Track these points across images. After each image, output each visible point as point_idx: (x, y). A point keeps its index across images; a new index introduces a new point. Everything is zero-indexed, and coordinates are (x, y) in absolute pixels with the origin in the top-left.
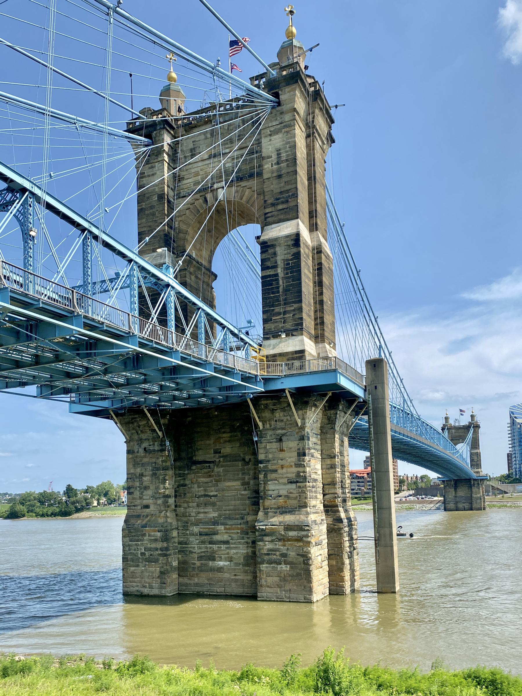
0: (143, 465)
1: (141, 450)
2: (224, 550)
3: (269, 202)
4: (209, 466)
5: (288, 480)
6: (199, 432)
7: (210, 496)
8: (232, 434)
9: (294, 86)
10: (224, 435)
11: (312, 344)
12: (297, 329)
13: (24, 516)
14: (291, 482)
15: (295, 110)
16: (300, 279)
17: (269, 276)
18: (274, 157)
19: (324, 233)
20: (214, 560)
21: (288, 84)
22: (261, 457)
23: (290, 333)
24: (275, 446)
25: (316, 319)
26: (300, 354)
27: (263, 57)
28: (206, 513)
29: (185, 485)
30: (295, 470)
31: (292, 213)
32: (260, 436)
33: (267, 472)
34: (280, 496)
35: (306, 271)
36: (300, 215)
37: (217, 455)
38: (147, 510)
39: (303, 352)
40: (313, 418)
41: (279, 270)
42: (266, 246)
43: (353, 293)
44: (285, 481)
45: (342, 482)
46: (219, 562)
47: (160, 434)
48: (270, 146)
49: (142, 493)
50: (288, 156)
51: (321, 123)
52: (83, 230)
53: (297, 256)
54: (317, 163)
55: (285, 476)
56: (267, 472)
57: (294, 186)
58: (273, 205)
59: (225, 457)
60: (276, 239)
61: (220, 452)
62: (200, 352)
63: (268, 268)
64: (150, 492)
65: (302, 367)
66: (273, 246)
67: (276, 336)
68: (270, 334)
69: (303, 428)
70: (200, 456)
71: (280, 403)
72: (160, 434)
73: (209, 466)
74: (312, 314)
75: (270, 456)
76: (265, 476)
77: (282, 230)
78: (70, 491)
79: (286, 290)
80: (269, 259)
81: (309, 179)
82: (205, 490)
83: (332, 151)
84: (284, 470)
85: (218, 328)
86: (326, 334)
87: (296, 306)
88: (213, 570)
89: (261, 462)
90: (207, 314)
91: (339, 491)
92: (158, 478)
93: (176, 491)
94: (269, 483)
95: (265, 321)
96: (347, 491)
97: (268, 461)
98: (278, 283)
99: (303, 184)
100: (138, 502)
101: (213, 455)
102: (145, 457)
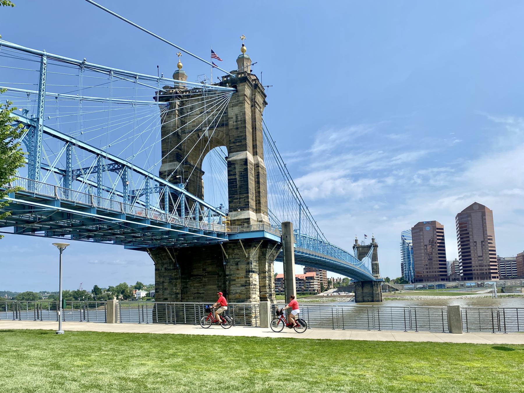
0: (164, 277)
1: (163, 269)
3: (232, 141)
7: (200, 293)
9: (244, 83)
10: (208, 261)
11: (254, 214)
12: (246, 207)
14: (243, 286)
15: (245, 95)
16: (248, 182)
17: (232, 179)
18: (234, 118)
19: (262, 156)
21: (241, 82)
22: (227, 273)
23: (242, 209)
24: (235, 267)
25: (256, 201)
26: (248, 220)
27: (229, 66)
29: (187, 288)
30: (244, 279)
31: (244, 148)
32: (227, 262)
33: (230, 280)
35: (251, 177)
36: (248, 148)
39: (249, 219)
40: (254, 253)
41: (237, 177)
42: (230, 165)
43: (282, 176)
45: (269, 285)
47: (174, 260)
48: (233, 112)
50: (241, 118)
51: (259, 99)
52: (146, 176)
53: (246, 170)
54: (257, 120)
56: (230, 280)
57: (244, 134)
58: (234, 143)
60: (236, 161)
62: (196, 225)
63: (231, 175)
64: (168, 291)
65: (248, 227)
66: (234, 164)
67: (236, 210)
68: (231, 209)
69: (248, 258)
70: (195, 272)
71: (237, 245)
72: (174, 260)
74: (254, 198)
75: (232, 272)
76: (229, 283)
77: (239, 156)
78: (96, 290)
79: (240, 187)
80: (232, 171)
81: (253, 129)
82: (198, 290)
83: (266, 110)
84: (239, 280)
85: (205, 209)
86: (262, 208)
87: (245, 195)
89: (227, 275)
90: (200, 203)
91: (268, 290)
92: (172, 284)
95: (230, 202)
96: (273, 290)
98: (236, 183)
99: (249, 132)
100: (161, 297)
102: (165, 272)
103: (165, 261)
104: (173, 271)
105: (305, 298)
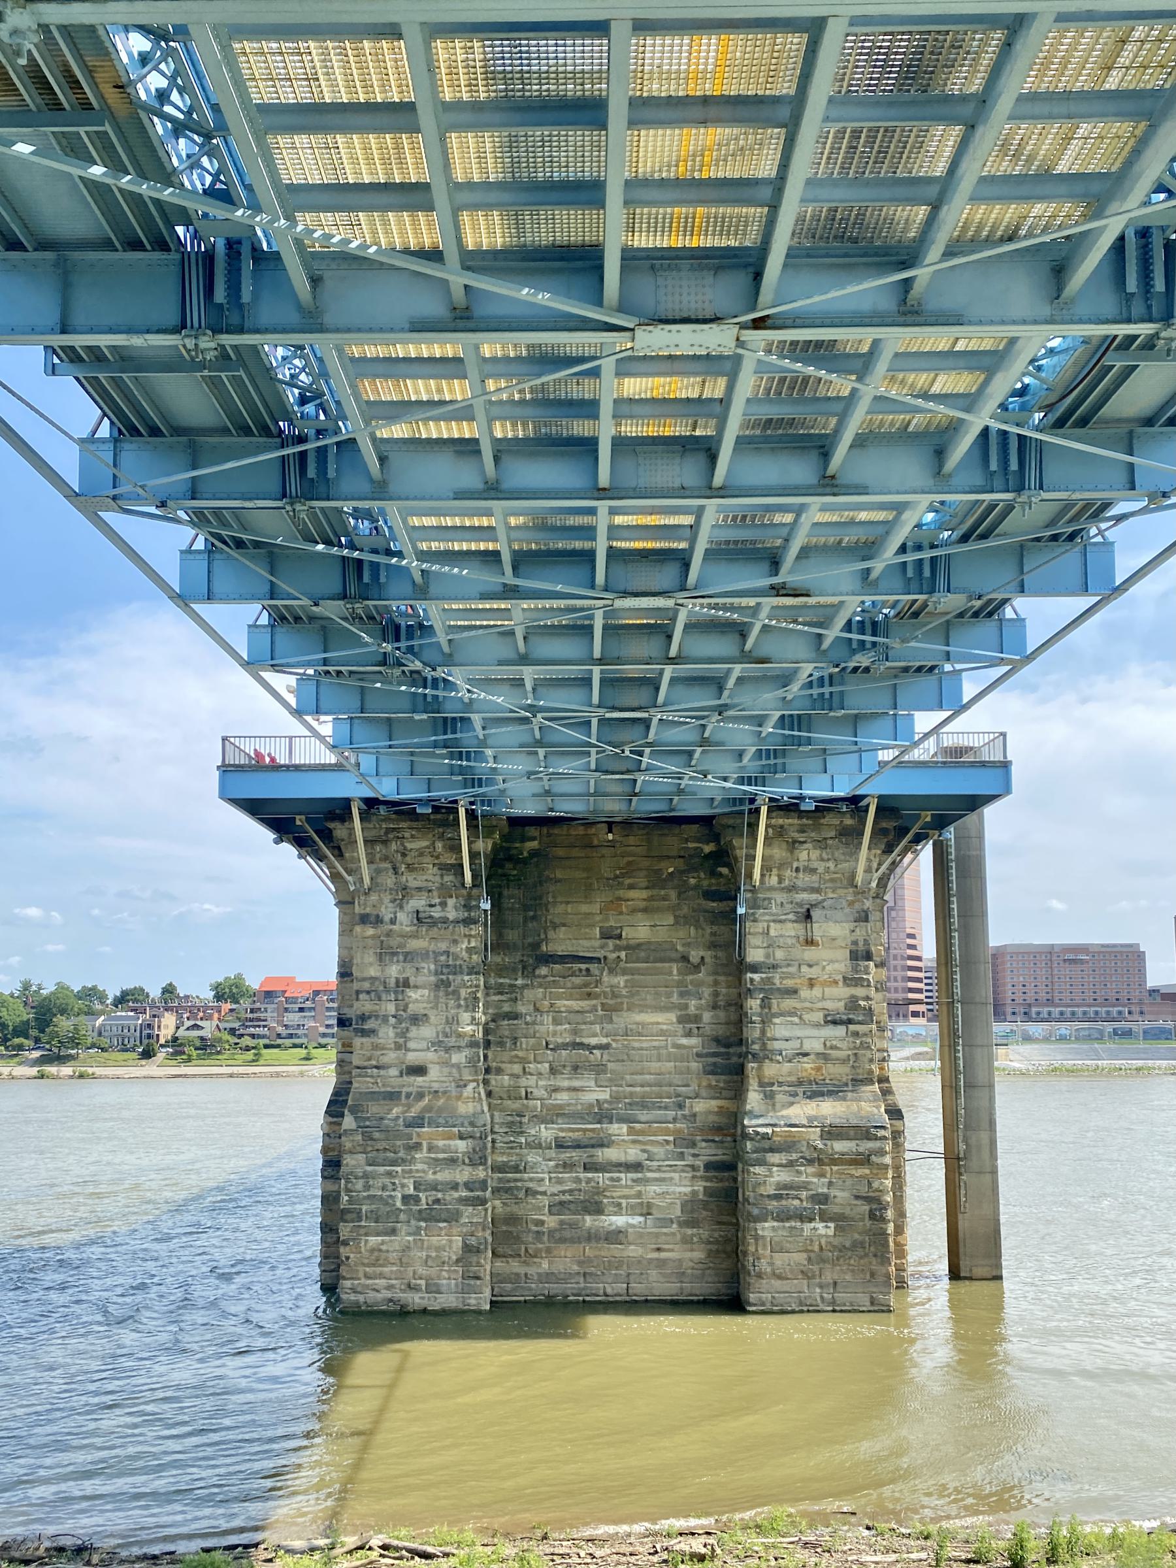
0: (409, 957)
2: (626, 1186)
4: (588, 970)
5: (826, 1016)
6: (560, 881)
7: (590, 1048)
8: (655, 892)
10: (633, 894)
14: (835, 1022)
20: (598, 1210)
22: (754, 955)
28: (575, 1089)
29: (515, 1016)
30: (844, 992)
32: (754, 905)
33: (769, 993)
34: (806, 1055)
37: (611, 943)
38: (420, 1079)
44: (819, 1017)
46: (614, 1218)
49: (404, 1034)
55: (820, 1005)
56: (769, 993)
59: (633, 948)
61: (620, 937)
64: (427, 1032)
70: (561, 942)
73: (588, 970)
75: (780, 954)
76: (766, 1003)
82: (575, 1032)
84: (817, 992)
88: (592, 1237)
89: (754, 968)
93: (487, 1031)
94: (776, 1020)
97: (774, 967)
100: (391, 1056)
101: (597, 943)
102: (415, 936)
103: (412, 880)
104: (462, 929)
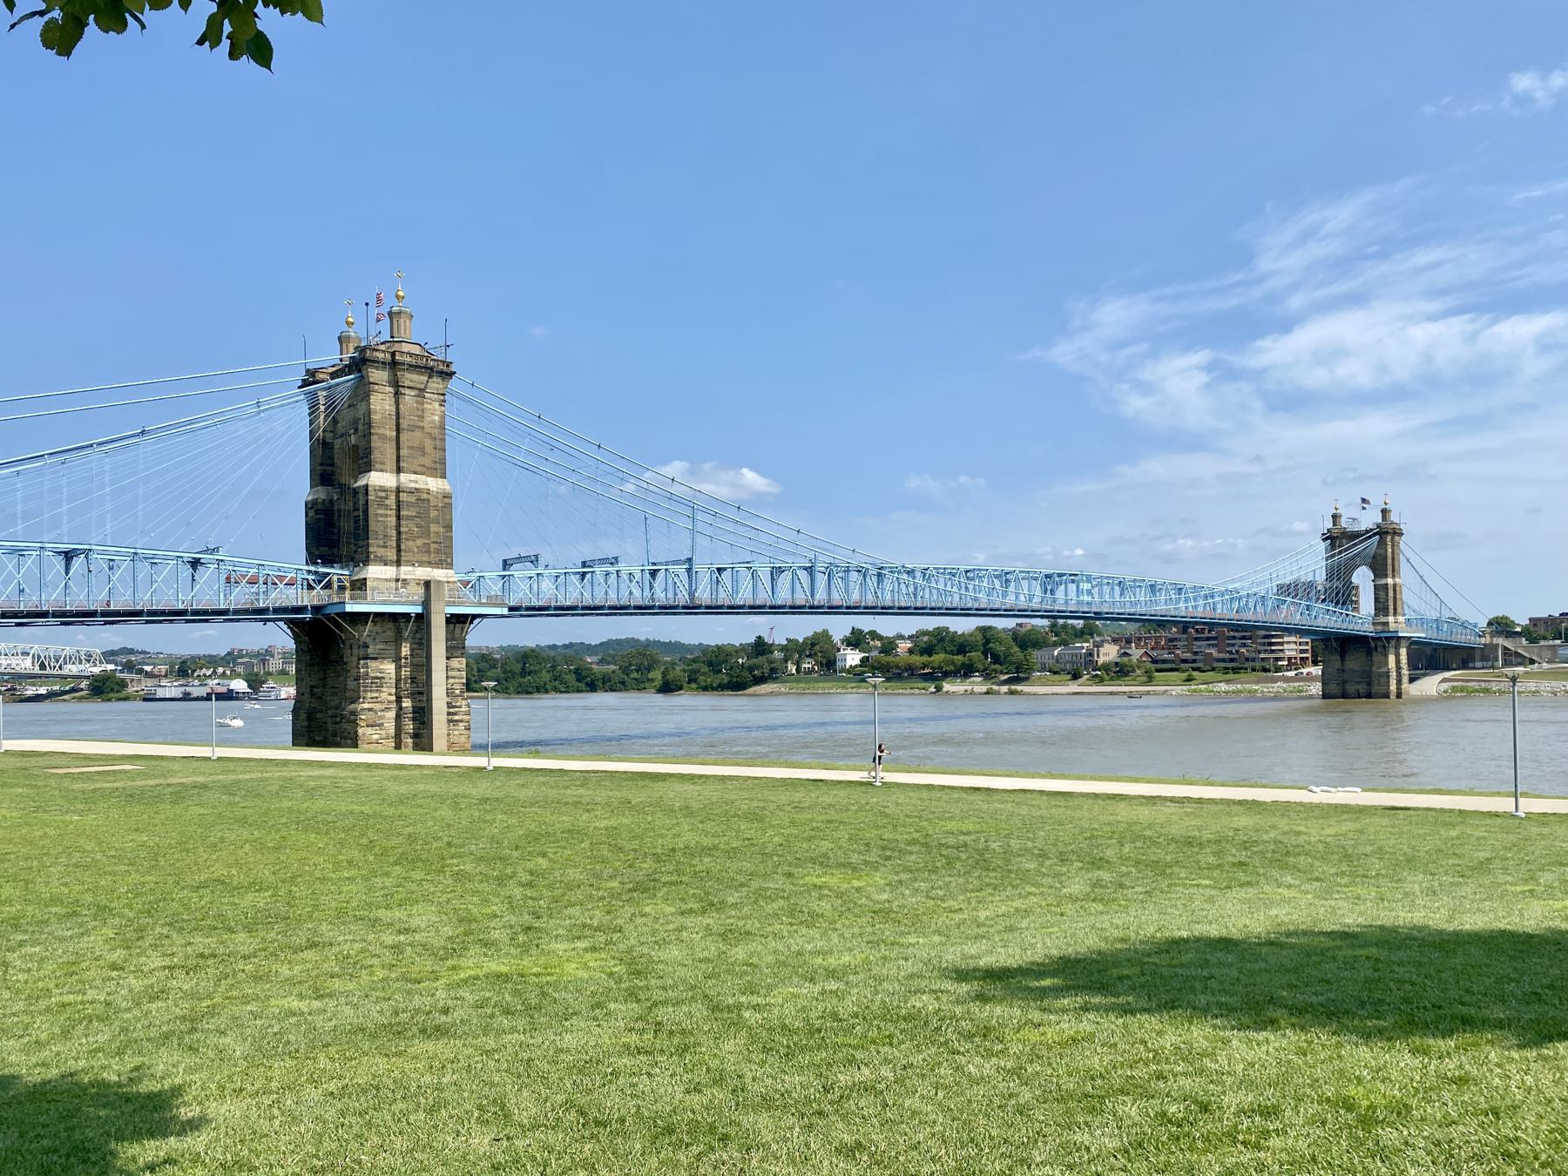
13: (680, 688)
105: (1228, 682)
